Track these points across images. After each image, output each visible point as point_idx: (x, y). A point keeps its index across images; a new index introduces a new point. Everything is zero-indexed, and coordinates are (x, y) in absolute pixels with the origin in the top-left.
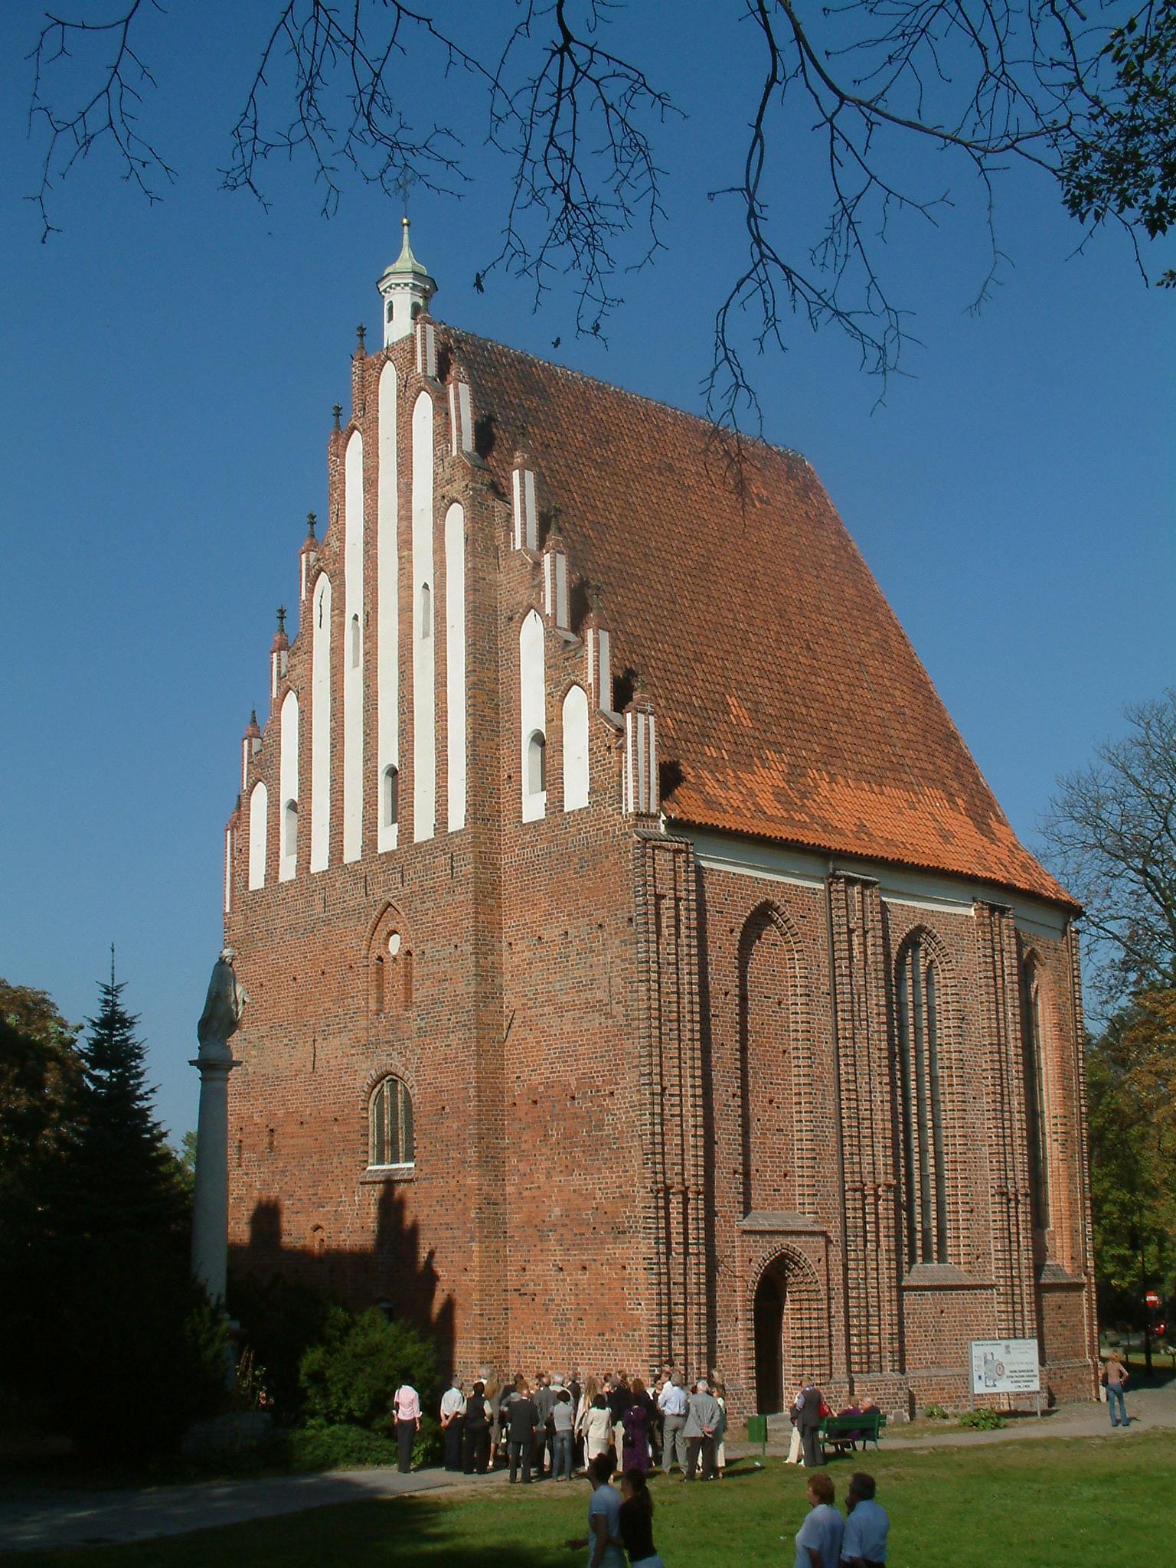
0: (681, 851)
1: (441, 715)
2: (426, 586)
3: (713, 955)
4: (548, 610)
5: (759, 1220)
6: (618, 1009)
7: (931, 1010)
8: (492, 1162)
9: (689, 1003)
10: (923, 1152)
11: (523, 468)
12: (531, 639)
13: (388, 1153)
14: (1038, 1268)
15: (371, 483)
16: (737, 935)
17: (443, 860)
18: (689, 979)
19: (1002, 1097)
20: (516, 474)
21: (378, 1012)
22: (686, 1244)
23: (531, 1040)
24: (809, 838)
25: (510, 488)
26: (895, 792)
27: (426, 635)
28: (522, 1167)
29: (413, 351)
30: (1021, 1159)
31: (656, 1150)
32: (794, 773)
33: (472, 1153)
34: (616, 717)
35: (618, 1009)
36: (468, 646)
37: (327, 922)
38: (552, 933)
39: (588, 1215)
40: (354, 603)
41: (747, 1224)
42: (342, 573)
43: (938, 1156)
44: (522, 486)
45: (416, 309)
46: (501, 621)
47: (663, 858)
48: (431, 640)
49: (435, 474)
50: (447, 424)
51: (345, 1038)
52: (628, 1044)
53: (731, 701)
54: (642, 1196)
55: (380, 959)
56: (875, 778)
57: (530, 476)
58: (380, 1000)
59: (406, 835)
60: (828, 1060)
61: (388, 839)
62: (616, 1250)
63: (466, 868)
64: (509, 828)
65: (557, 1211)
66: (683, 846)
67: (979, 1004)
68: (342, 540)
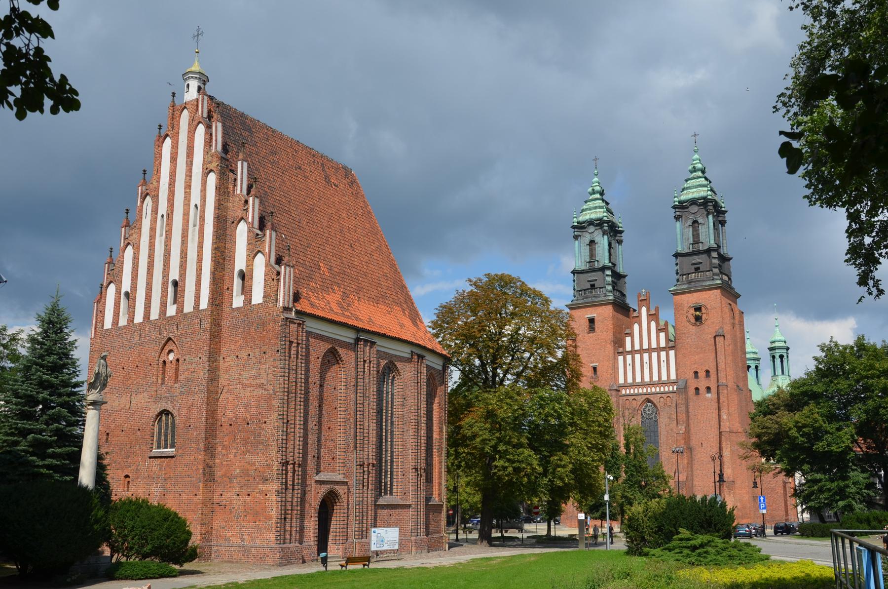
1: (200, 260)
2: (196, 206)
3: (311, 366)
4: (250, 220)
5: (322, 477)
6: (270, 387)
7: (392, 395)
8: (210, 449)
9: (301, 386)
10: (386, 451)
11: (243, 160)
12: (242, 232)
13: (163, 443)
14: (428, 499)
15: (174, 159)
17: (197, 321)
18: (301, 376)
19: (418, 431)
20: (239, 163)
21: (162, 384)
22: (293, 485)
23: (231, 399)
24: (350, 322)
25: (237, 168)
26: (383, 307)
27: (195, 226)
28: (224, 452)
29: (197, 106)
30: (423, 454)
31: (283, 448)
32: (345, 296)
33: (202, 445)
34: (277, 267)
35: (270, 387)
36: (214, 232)
37: (140, 344)
38: (243, 354)
39: (252, 473)
40: (163, 209)
41: (317, 478)
42: (158, 196)
43: (392, 452)
44: (242, 169)
45: (199, 88)
46: (229, 223)
47: (294, 327)
48: (197, 228)
49: (204, 158)
50: (211, 139)
51: (145, 394)
52: (274, 402)
53: (321, 265)
54: (276, 466)
55: (164, 362)
56: (376, 300)
57: (245, 164)
58: (163, 379)
59: (180, 310)
60: (352, 412)
61: (171, 310)
62: (262, 487)
63: (207, 325)
64: (227, 310)
65: (238, 471)
67: (411, 392)
68: (158, 182)
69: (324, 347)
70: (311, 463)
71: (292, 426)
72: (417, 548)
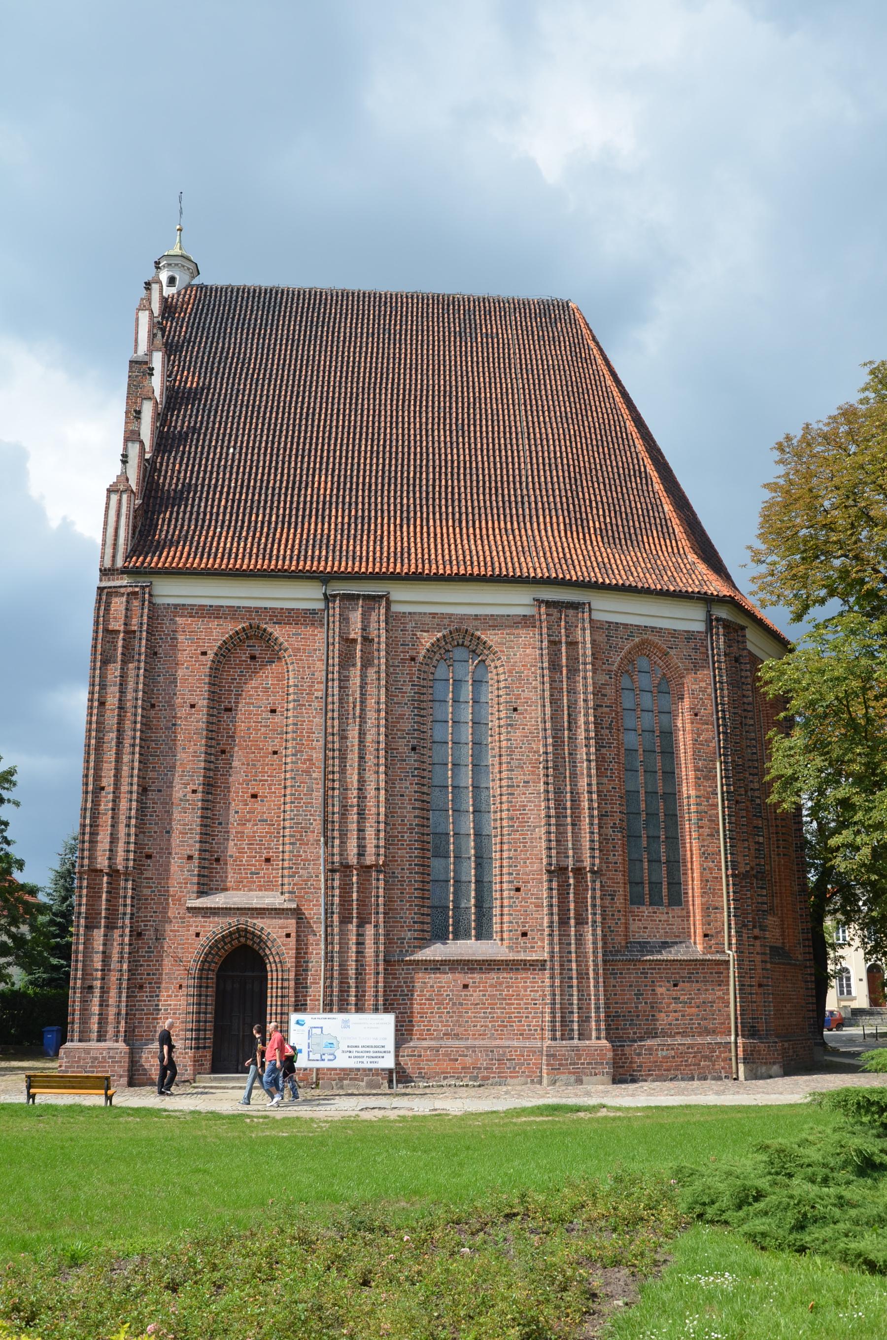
0: (136, 593)
5: (218, 900)
16: (211, 655)
66: (137, 589)
69: (219, 632)
70: (181, 873)
71: (111, 797)
72: (554, 1070)
